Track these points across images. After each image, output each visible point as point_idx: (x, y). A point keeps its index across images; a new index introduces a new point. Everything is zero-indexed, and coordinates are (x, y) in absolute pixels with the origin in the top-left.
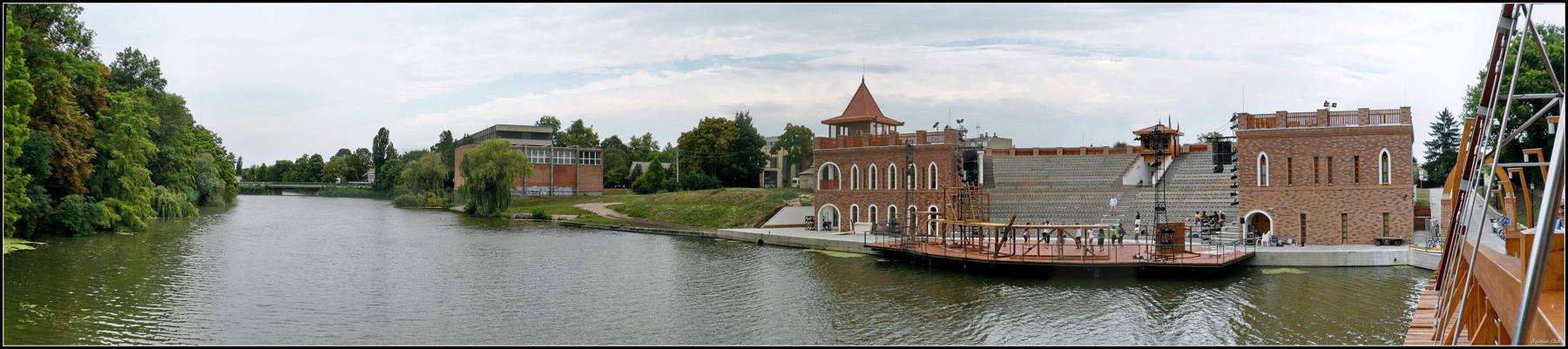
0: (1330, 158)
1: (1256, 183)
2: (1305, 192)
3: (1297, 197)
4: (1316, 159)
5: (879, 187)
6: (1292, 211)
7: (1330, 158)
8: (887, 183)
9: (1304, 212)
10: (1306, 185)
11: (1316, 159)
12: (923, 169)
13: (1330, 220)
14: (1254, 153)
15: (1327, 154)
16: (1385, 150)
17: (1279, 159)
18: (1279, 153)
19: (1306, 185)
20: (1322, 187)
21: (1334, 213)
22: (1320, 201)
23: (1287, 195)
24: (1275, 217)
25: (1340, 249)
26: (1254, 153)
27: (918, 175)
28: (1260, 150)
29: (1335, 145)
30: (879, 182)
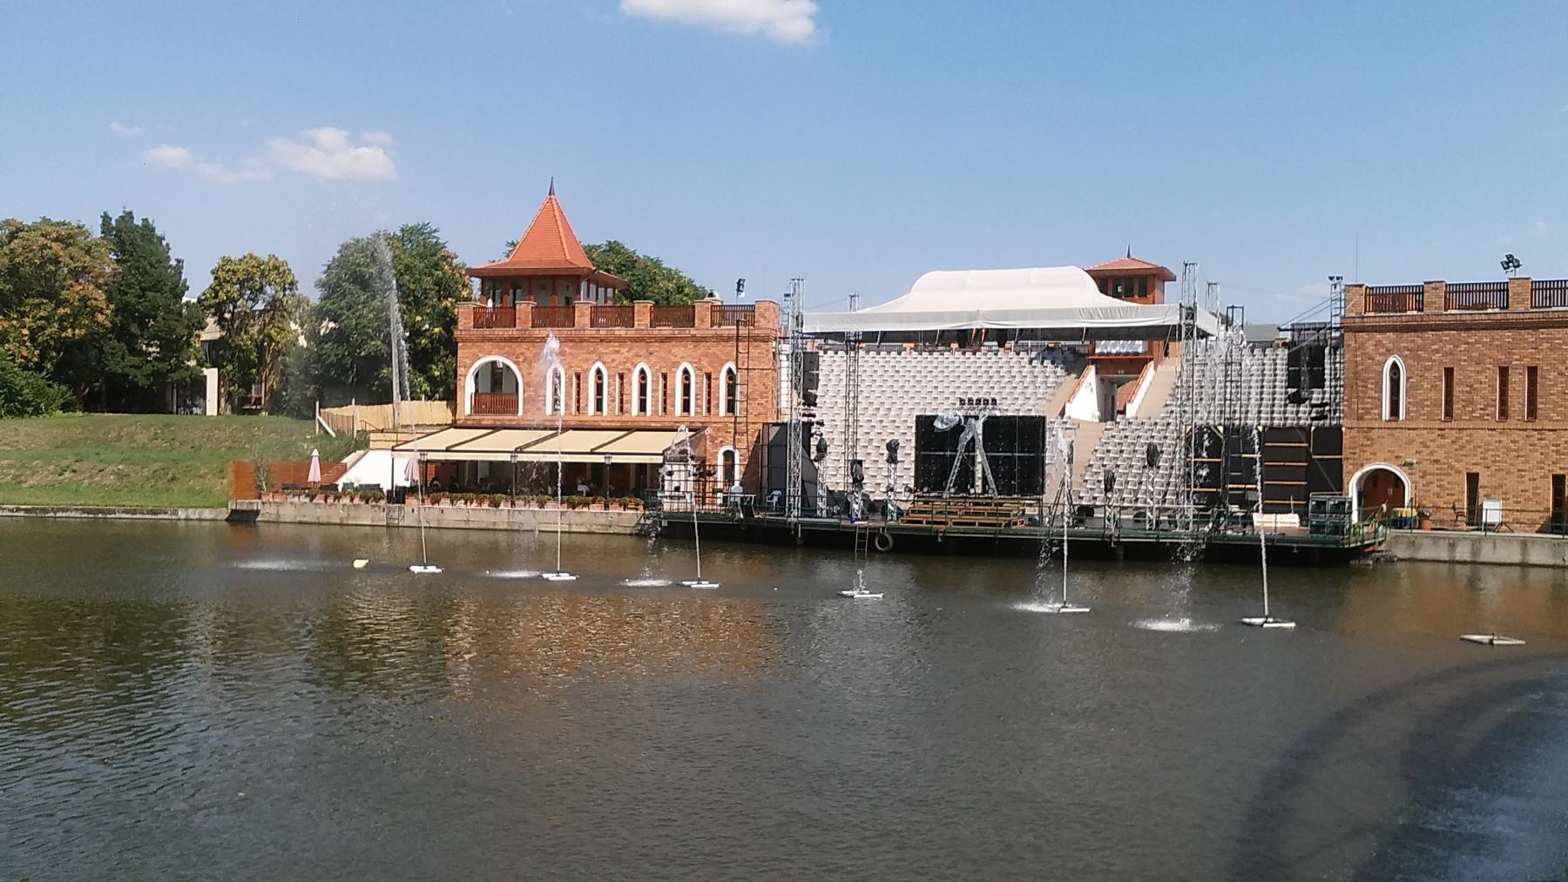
0: (1532, 371)
1: (1380, 415)
2: (1478, 434)
3: (1461, 442)
4: (1504, 372)
5: (611, 410)
6: (1452, 468)
7: (1532, 371)
8: (629, 402)
9: (1475, 470)
10: (1481, 418)
11: (1504, 372)
12: (709, 377)
13: (1529, 485)
14: (1378, 358)
15: (1527, 361)
16: (599, 365)
17: (1428, 369)
18: (1430, 360)
19: (1481, 418)
20: (1512, 423)
21: (1538, 474)
22: (1509, 450)
23: (1442, 436)
24: (1416, 477)
25: (588, 471)
26: (1378, 358)
27: (699, 389)
28: (1389, 352)
29: (1546, 345)
30: (655, 399)
